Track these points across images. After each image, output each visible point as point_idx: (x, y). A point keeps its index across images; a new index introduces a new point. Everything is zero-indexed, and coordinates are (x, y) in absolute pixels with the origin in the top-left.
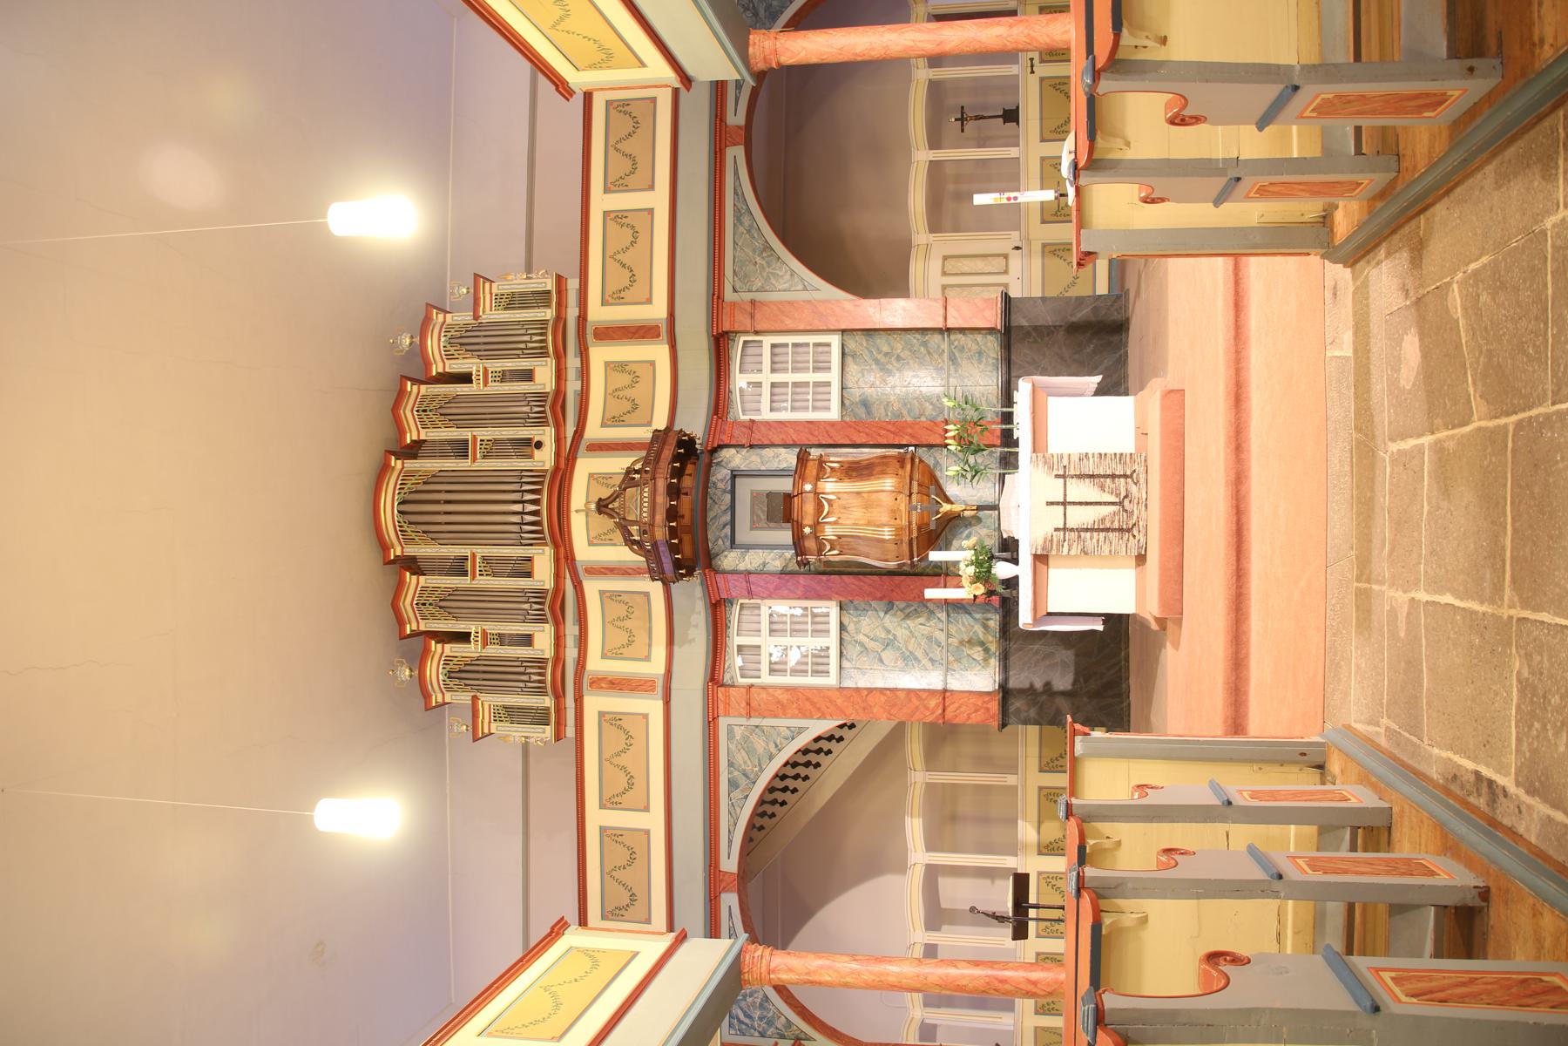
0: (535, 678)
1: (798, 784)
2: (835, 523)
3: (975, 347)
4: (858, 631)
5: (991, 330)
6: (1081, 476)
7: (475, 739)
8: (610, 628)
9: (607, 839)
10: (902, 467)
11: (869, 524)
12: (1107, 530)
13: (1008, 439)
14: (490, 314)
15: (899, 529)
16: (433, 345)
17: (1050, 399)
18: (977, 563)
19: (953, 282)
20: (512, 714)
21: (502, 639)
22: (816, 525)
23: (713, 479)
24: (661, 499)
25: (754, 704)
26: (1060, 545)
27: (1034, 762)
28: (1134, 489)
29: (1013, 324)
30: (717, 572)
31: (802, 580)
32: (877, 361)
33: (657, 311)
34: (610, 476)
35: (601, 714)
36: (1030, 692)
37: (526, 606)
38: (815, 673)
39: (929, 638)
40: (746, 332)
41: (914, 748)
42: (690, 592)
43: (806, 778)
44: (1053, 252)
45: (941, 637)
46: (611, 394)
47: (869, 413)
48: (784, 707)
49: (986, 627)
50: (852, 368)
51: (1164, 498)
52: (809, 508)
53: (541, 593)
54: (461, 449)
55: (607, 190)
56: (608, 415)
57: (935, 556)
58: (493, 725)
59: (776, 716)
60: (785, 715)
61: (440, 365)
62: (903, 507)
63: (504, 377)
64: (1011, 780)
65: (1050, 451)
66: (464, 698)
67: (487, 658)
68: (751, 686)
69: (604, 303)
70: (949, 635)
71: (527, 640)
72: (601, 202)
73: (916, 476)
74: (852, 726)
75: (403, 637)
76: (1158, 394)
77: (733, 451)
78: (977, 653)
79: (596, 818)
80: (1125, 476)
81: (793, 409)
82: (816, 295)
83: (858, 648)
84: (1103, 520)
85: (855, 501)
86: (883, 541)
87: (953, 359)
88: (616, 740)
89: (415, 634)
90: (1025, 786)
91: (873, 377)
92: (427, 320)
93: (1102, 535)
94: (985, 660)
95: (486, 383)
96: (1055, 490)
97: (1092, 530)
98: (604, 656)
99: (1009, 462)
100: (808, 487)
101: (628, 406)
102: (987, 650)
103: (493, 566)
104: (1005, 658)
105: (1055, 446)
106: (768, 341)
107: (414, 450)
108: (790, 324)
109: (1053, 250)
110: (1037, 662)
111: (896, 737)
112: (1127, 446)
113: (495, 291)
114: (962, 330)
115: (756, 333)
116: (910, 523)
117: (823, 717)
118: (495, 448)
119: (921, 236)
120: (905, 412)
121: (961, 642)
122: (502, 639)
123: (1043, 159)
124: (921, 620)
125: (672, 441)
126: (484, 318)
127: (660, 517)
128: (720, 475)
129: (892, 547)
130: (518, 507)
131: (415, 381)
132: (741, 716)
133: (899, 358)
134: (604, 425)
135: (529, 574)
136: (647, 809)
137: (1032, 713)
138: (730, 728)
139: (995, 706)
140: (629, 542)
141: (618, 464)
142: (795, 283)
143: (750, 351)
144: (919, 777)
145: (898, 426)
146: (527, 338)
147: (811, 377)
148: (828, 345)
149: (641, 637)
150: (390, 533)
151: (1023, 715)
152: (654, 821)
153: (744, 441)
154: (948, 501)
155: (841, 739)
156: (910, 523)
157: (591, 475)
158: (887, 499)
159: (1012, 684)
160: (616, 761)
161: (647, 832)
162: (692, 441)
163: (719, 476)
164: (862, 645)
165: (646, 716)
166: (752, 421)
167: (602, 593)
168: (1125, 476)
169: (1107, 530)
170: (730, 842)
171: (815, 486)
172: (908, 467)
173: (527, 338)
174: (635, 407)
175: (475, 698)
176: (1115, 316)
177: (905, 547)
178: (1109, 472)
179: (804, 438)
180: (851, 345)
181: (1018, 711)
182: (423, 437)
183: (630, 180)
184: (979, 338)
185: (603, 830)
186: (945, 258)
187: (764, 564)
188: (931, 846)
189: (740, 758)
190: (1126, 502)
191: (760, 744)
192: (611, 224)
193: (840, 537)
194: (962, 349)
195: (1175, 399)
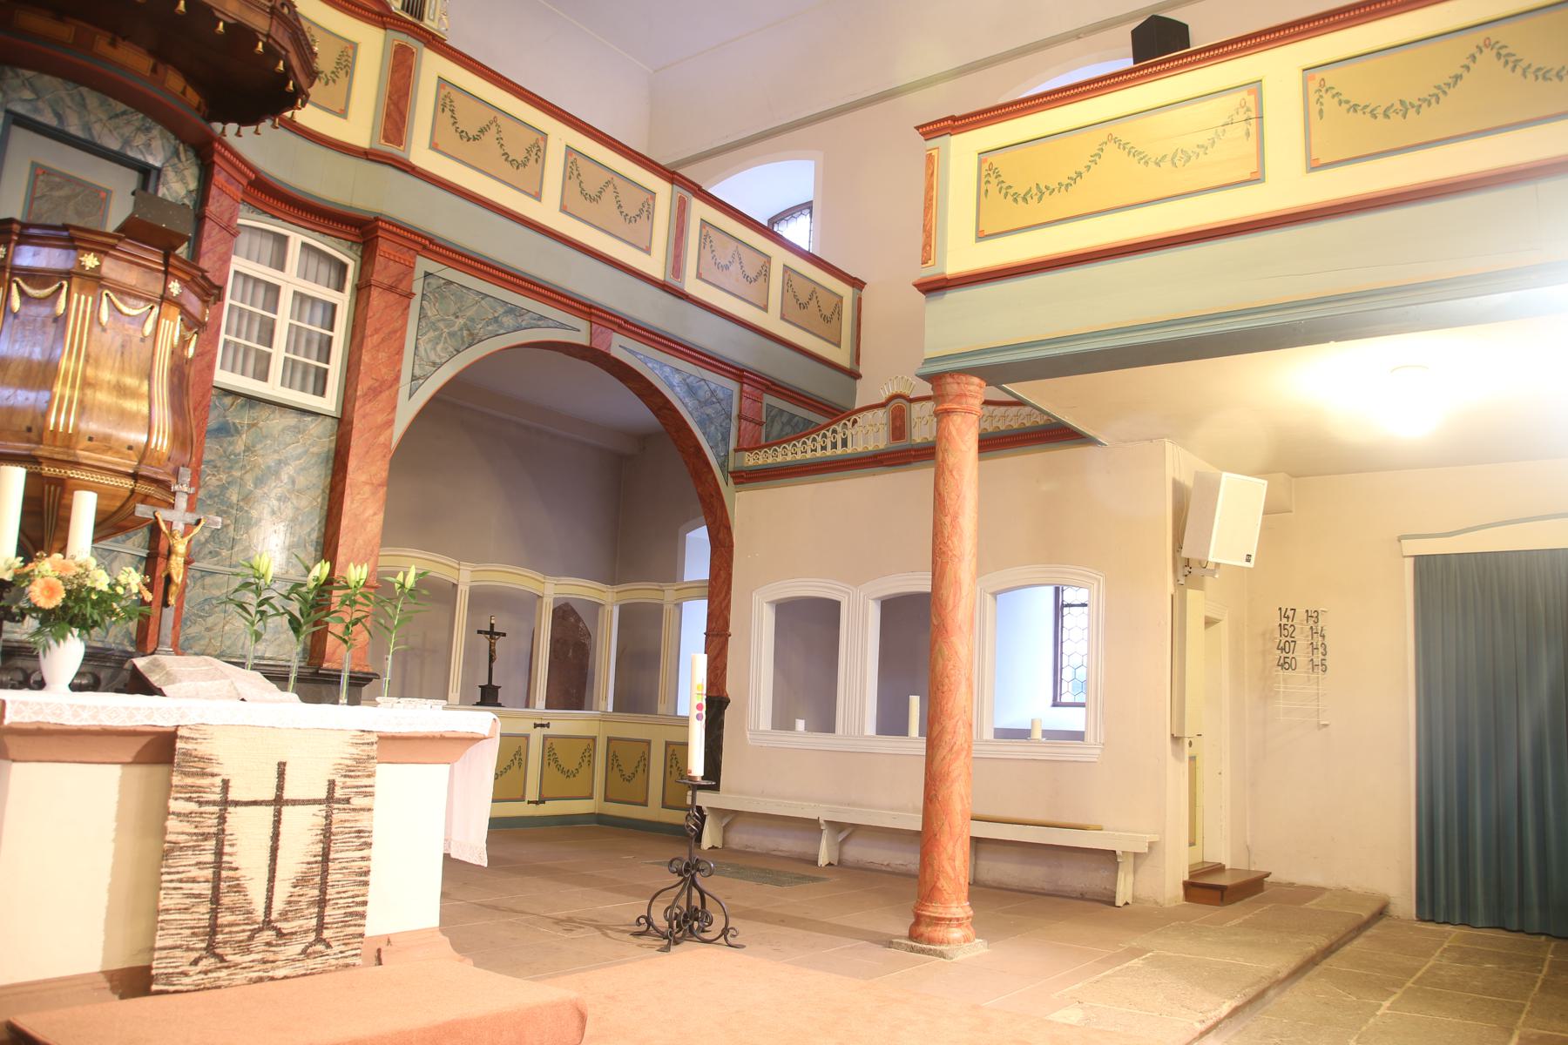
2: (95, 318)
6: (327, 835)
12: (215, 899)
23: (156, 131)
26: (193, 794)
28: (294, 949)
33: (420, 154)
62: (109, 459)
72: (560, 136)
76: (573, 995)
77: (193, 185)
80: (321, 927)
84: (238, 888)
93: (205, 889)
96: (306, 782)
97: (218, 865)
100: (175, 287)
105: (389, 778)
106: (343, 301)
116: (76, 464)
147: (279, 352)
148: (320, 390)
162: (249, 116)
169: (215, 899)
178: (331, 893)
183: (574, 184)
190: (268, 935)
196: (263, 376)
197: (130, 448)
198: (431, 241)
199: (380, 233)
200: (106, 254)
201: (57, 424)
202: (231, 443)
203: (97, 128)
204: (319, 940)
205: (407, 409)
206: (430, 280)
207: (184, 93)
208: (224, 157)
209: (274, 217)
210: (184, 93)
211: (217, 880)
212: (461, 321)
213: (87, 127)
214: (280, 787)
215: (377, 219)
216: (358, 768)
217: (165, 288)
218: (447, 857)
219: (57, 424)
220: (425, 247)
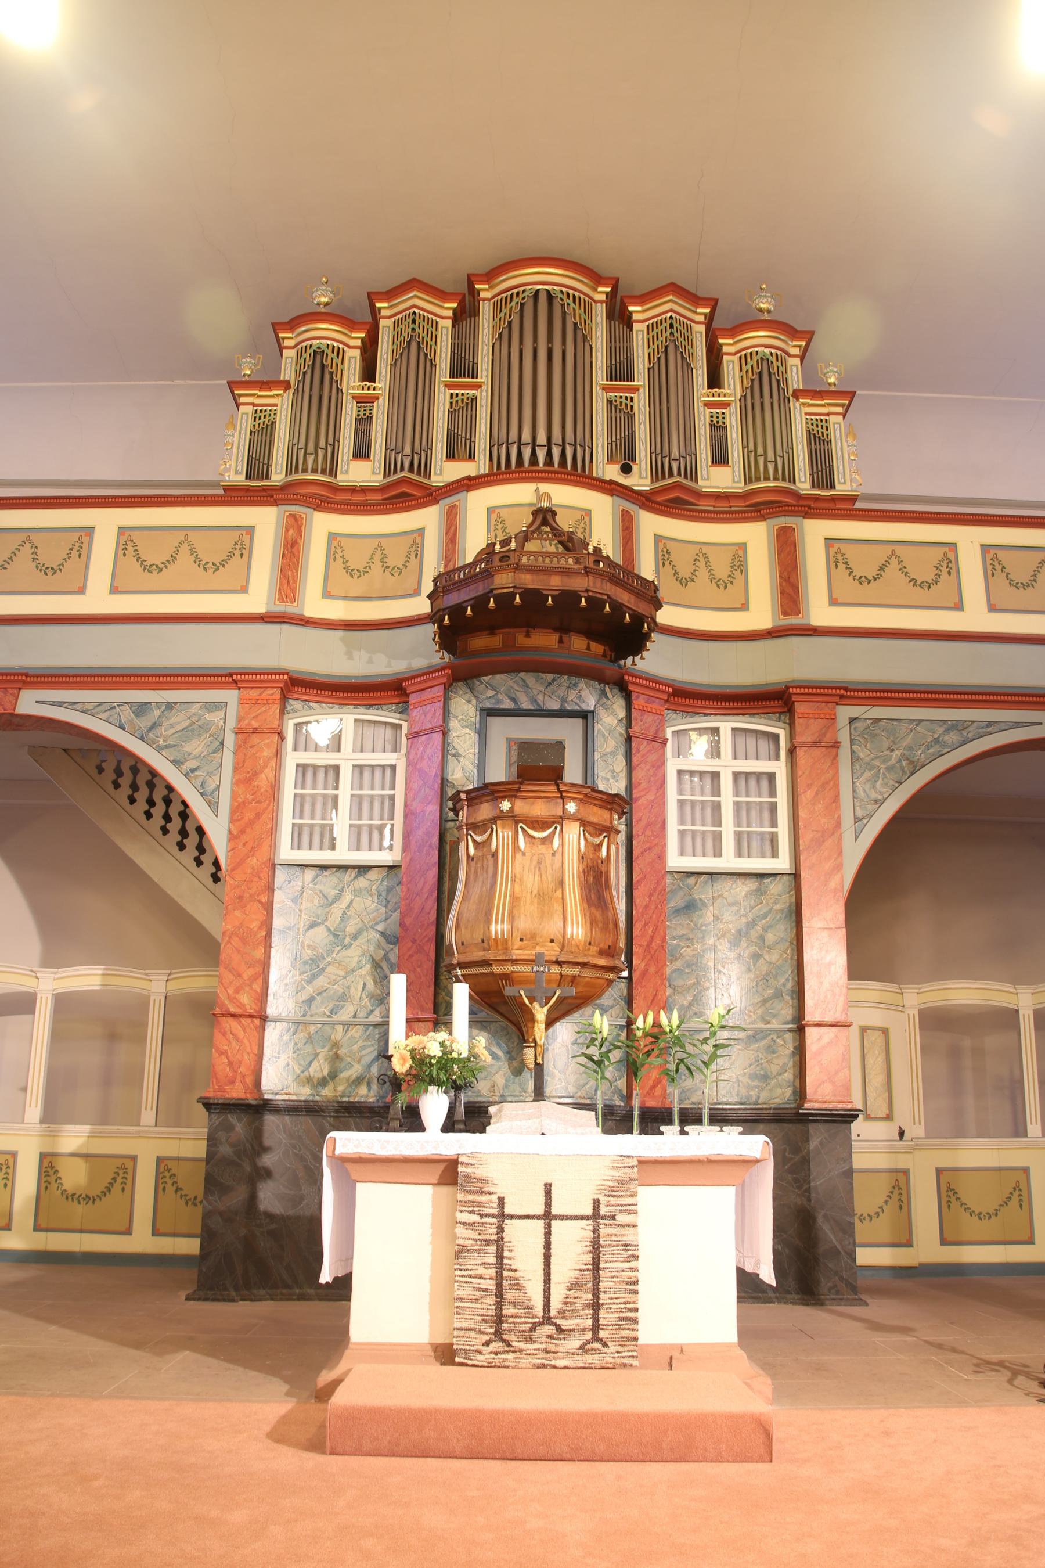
0: (310, 459)
1: (158, 820)
2: (516, 848)
3: (774, 1069)
4: (357, 893)
5: (801, 1093)
6: (596, 1246)
7: (232, 385)
8: (374, 543)
9: (75, 536)
10: (602, 953)
11: (515, 899)
12: (499, 1294)
13: (654, 1120)
15: (504, 944)
16: (758, 338)
17: (732, 1190)
18: (446, 1062)
19: (861, 1037)
21: (364, 421)
22: (513, 818)
23: (582, 683)
24: (556, 583)
25: (255, 739)
26: (474, 1207)
27: (171, 1149)
28: (573, 1344)
29: (812, 1128)
30: (447, 688)
31: (433, 809)
32: (752, 924)
33: (820, 612)
34: (588, 528)
35: (250, 530)
36: (257, 1146)
37: (408, 450)
38: (298, 830)
39: (344, 998)
40: (791, 736)
41: (195, 981)
42: (420, 650)
43: (165, 831)
44: (896, 1186)
45: (346, 1015)
46: (701, 552)
47: (677, 911)
48: (248, 781)
49: (358, 1081)
50: (741, 889)
51: (560, 1421)
52: (540, 809)
53: (425, 470)
54: (621, 371)
55: (985, 548)
56: (671, 546)
57: (461, 994)
58: (249, 409)
59: (236, 769)
60: (236, 783)
61: (732, 349)
63: (718, 429)
64: (148, 1117)
65: (641, 1190)
66: (288, 372)
67: (339, 403)
68: (281, 737)
69: (829, 542)
70: (347, 1026)
71: (362, 452)
72: (968, 541)
73: (588, 973)
74: (216, 879)
75: (372, 297)
77: (622, 713)
78: (320, 1068)
79: (106, 522)
80: (596, 1328)
81: (681, 803)
82: (848, 835)
83: (334, 892)
84: (518, 1287)
85: (549, 878)
86: (488, 921)
87: (756, 1036)
88: (211, 549)
89: (375, 313)
90: (138, 1136)
91: (732, 920)
92: (792, 332)
93: (491, 1285)
94: (309, 1080)
95: (708, 405)
97: (500, 1266)
98: (332, 536)
99: (616, 1120)
100: (571, 807)
101: (685, 572)
102: (323, 1082)
103: (462, 412)
104: (296, 1109)
105: (652, 1200)
106: (780, 768)
107: (619, 315)
108: (806, 797)
109: (899, 1183)
110: (302, 1159)
111: (204, 948)
112: (651, 1331)
113: (832, 419)
114: (800, 1050)
115: (791, 751)
116: (514, 962)
117: (232, 837)
118: (621, 415)
119: (916, 997)
120: (678, 964)
121: (336, 1045)
122: (364, 421)
123: (1026, 1170)
124: (370, 985)
125: (642, 608)
126: (795, 405)
127: (529, 581)
128: (588, 697)
129: (478, 936)
130: (542, 439)
131: (710, 319)
132: (239, 720)
133: (756, 956)
134: (658, 539)
135: (451, 455)
136: (114, 590)
137: (225, 1150)
138: (222, 705)
139: (237, 1092)
140: (488, 552)
141: (603, 536)
142: (863, 811)
143: (764, 745)
144: (156, 987)
145: (659, 954)
146: (771, 456)
147: (728, 829)
148: (774, 854)
149: (357, 586)
151: (222, 1136)
152: (97, 599)
153: (636, 728)
154: (549, 1023)
155: (199, 862)
156: (514, 962)
157: (588, 513)
158: (553, 927)
159: (270, 1120)
160: (185, 549)
161: (81, 591)
163: (585, 693)
164: (338, 898)
165: (244, 589)
166: (664, 743)
167: (421, 532)
168: (596, 1328)
169: (499, 1294)
170: (60, 704)
171: (574, 818)
172: (602, 962)
173: (771, 456)
174: (683, 582)
175: (286, 385)
176: (825, 1284)
177: (478, 955)
178: (604, 1298)
179: (641, 811)
180: (776, 888)
181: (230, 1128)
182: (636, 326)
183: (1000, 579)
184: (789, 1076)
185: (90, 531)
186: (885, 1031)
187: (456, 756)
188: (63, 1002)
189: (179, 720)
190: (549, 1329)
191: (196, 747)
192: (939, 552)
193: (495, 855)
194: (771, 1050)
195: (756, 1441)
196: (718, 853)
197: (552, 941)
198: (846, 689)
199: (794, 698)
200: (516, 797)
201: (496, 932)
202: (701, 917)
203: (540, 698)
204: (596, 1338)
205: (854, 852)
206: (857, 724)
207: (588, 648)
208: (637, 684)
209: (706, 715)
210: (588, 648)
211: (499, 1279)
212: (898, 753)
213: (534, 700)
214: (548, 1204)
215: (788, 687)
216: (620, 1188)
217: (564, 809)
218: (741, 1273)
219: (496, 932)
220: (842, 697)
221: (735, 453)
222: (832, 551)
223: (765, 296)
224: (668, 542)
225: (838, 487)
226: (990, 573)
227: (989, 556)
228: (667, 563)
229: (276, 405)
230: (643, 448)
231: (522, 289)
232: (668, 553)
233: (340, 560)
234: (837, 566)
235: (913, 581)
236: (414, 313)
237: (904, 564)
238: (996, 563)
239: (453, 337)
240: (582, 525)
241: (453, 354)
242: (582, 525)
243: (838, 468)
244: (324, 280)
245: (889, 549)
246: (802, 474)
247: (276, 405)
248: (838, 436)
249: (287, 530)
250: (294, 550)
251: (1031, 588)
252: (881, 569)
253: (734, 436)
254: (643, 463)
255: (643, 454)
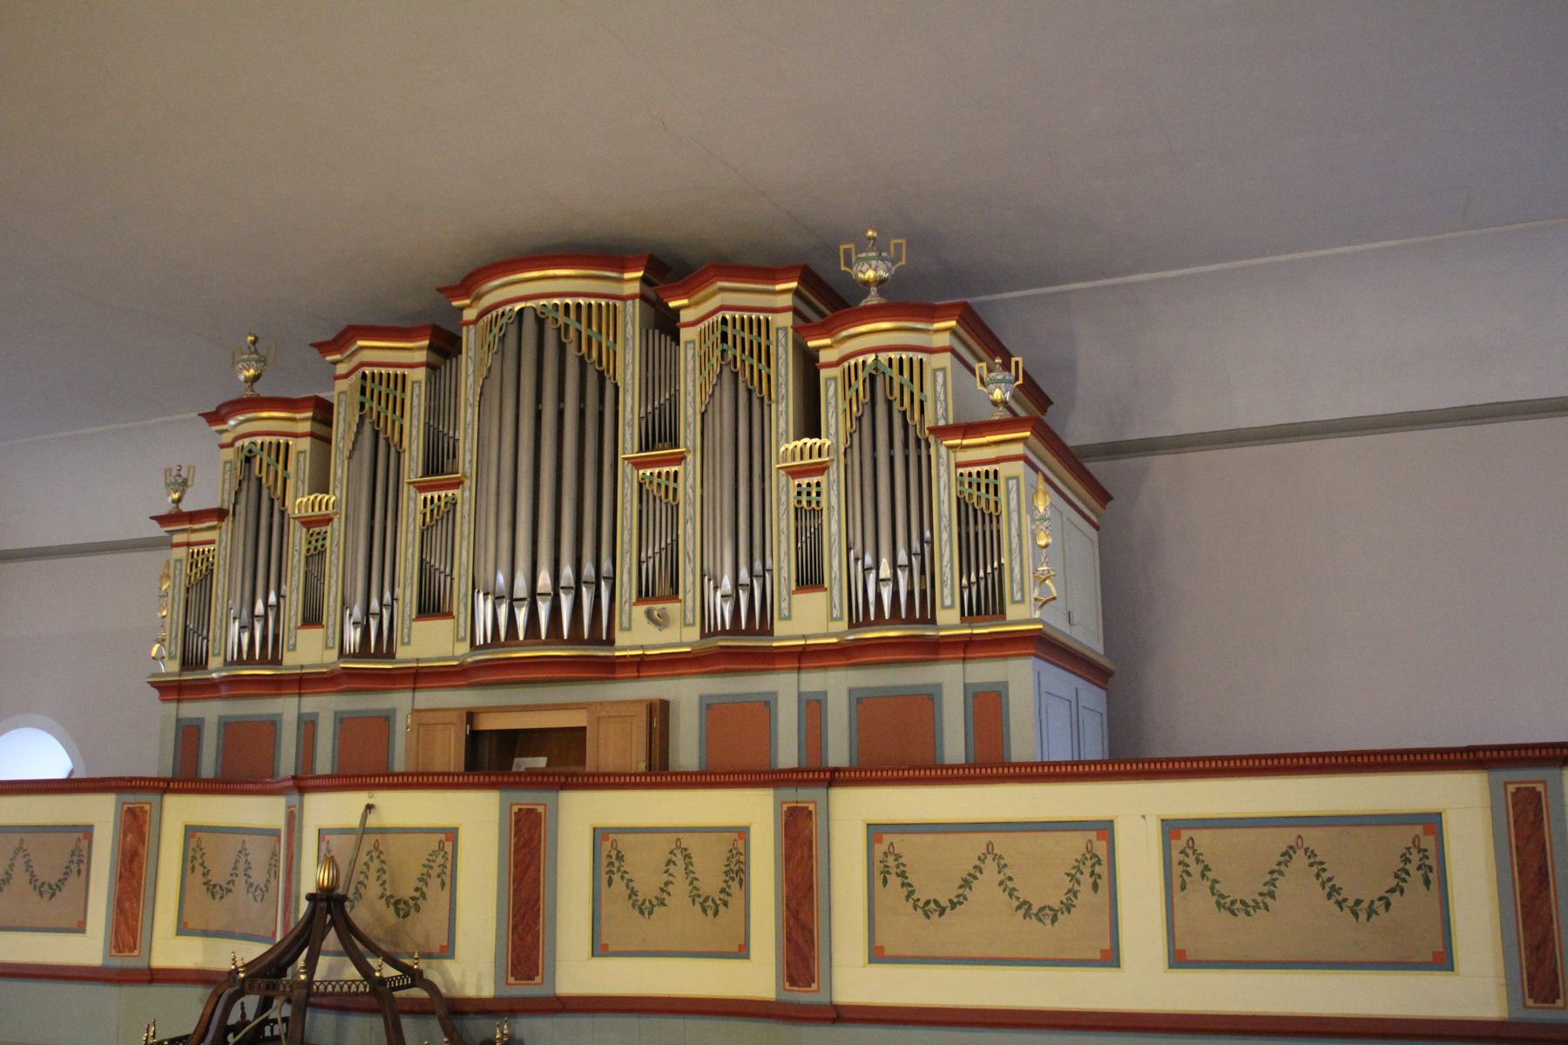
14: (948, 466)
16: (872, 337)
20: (200, 586)
55: (1171, 829)
69: (876, 832)
95: (795, 473)
98: (191, 831)
113: (1004, 469)
150: (498, 291)
174: (645, 909)
182: (686, 334)
183: (1198, 900)
192: (1076, 843)
221: (833, 565)
222: (880, 849)
223: (866, 260)
224: (620, 837)
225: (1012, 612)
226: (1177, 882)
227: (1177, 845)
228: (616, 877)
229: (212, 542)
230: (689, 569)
231: (500, 310)
232: (620, 857)
233: (199, 870)
234: (885, 881)
235: (1025, 905)
236: (364, 376)
237: (1008, 872)
238: (1191, 860)
239: (429, 398)
240: (440, 860)
241: (428, 426)
242: (440, 860)
243: (1012, 570)
244: (250, 338)
245: (983, 838)
246: (947, 591)
247: (212, 542)
248: (1013, 503)
249: (125, 836)
250: (135, 866)
251: (1262, 912)
252: (966, 883)
253: (834, 528)
254: (690, 596)
255: (689, 580)
